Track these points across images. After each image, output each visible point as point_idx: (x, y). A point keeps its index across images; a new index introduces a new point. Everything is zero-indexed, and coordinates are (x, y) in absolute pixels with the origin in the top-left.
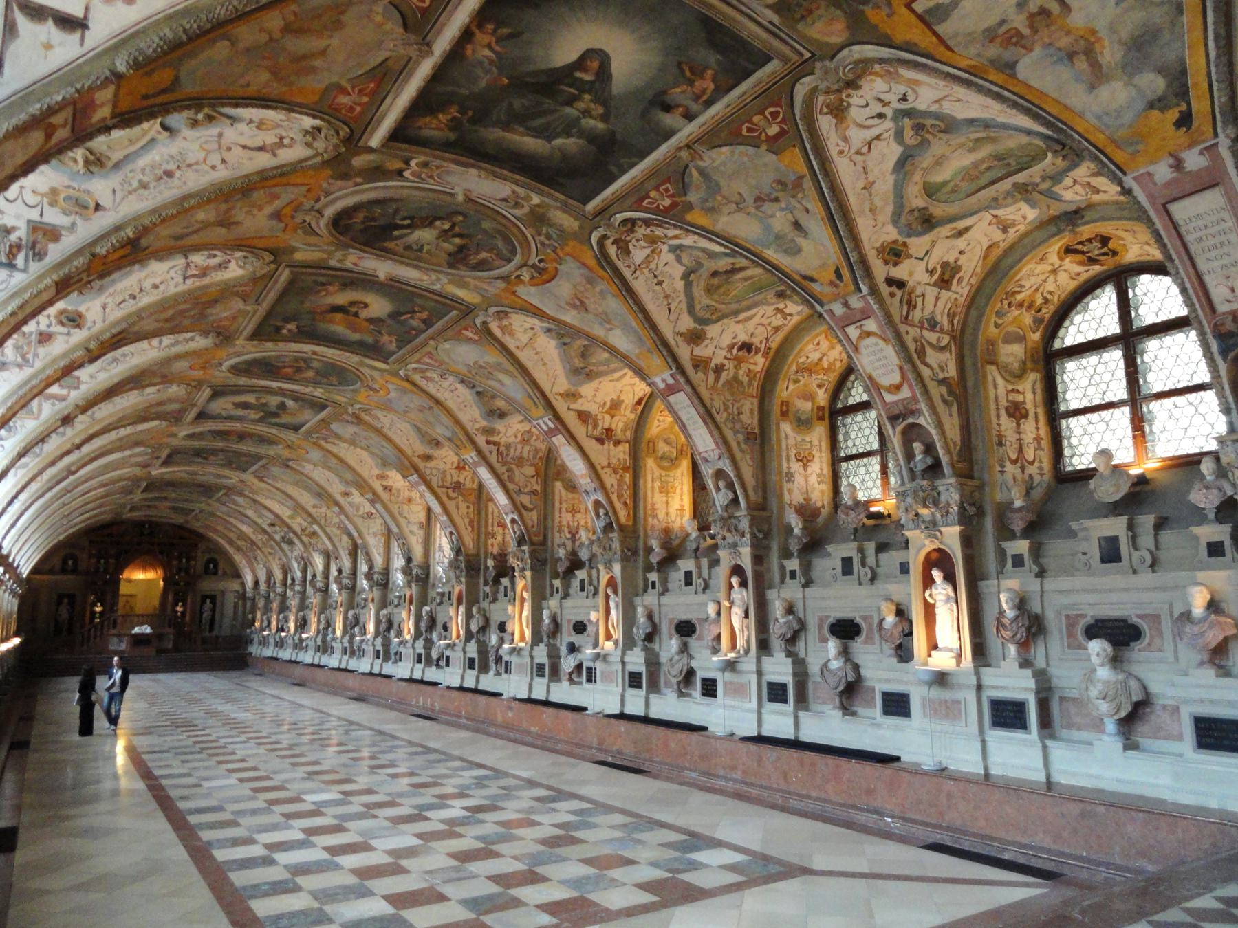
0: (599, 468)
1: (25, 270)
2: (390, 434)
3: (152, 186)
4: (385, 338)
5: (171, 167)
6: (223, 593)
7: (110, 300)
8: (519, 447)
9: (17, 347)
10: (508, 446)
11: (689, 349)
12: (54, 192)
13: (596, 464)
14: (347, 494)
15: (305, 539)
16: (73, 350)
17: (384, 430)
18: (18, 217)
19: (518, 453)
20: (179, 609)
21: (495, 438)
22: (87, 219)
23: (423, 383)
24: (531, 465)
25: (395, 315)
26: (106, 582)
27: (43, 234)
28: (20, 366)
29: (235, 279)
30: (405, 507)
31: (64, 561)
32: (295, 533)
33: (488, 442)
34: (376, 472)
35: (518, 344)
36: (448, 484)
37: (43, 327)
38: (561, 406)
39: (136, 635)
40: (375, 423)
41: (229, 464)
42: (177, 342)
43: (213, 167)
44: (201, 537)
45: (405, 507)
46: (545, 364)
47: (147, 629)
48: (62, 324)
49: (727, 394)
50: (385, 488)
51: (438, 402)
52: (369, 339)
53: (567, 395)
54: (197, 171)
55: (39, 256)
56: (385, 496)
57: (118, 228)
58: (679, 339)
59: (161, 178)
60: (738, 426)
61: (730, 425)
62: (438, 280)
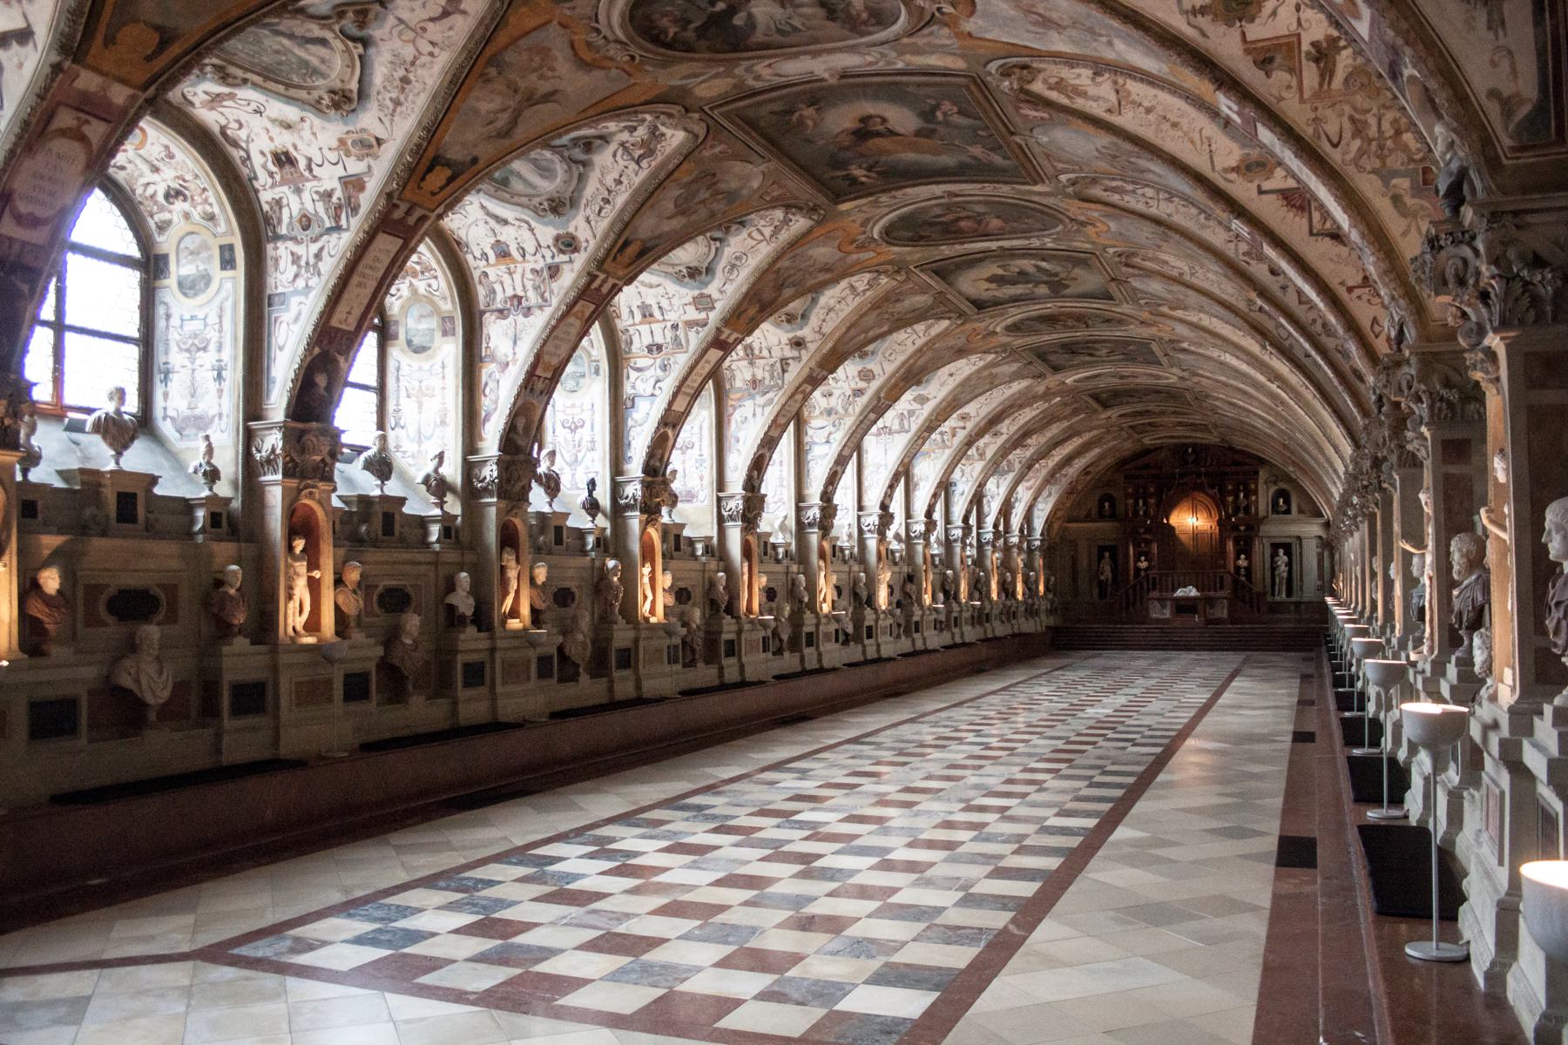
0: (1342, 292)
1: (347, 229)
2: (1194, 281)
3: (402, 98)
4: (977, 151)
5: (401, 73)
6: (1299, 538)
7: (588, 211)
9: (536, 288)
11: (1235, 33)
12: (342, 142)
13: (1333, 282)
17: (1187, 277)
18: (331, 178)
20: (1242, 562)
22: (376, 157)
23: (1115, 198)
25: (928, 115)
26: (1149, 530)
27: (353, 184)
28: (541, 308)
29: (681, 145)
31: (1101, 506)
35: (1106, 106)
37: (549, 261)
38: (1243, 190)
40: (1165, 269)
42: (777, 230)
43: (431, 54)
44: (1262, 462)
46: (1175, 125)
47: (1192, 592)
48: (563, 252)
49: (1360, 99)
51: (1157, 221)
52: (964, 158)
53: (1249, 168)
54: (424, 65)
55: (355, 210)
57: (401, 155)
58: (1202, 21)
59: (403, 89)
60: (1396, 161)
61: (1372, 163)
62: (883, 55)
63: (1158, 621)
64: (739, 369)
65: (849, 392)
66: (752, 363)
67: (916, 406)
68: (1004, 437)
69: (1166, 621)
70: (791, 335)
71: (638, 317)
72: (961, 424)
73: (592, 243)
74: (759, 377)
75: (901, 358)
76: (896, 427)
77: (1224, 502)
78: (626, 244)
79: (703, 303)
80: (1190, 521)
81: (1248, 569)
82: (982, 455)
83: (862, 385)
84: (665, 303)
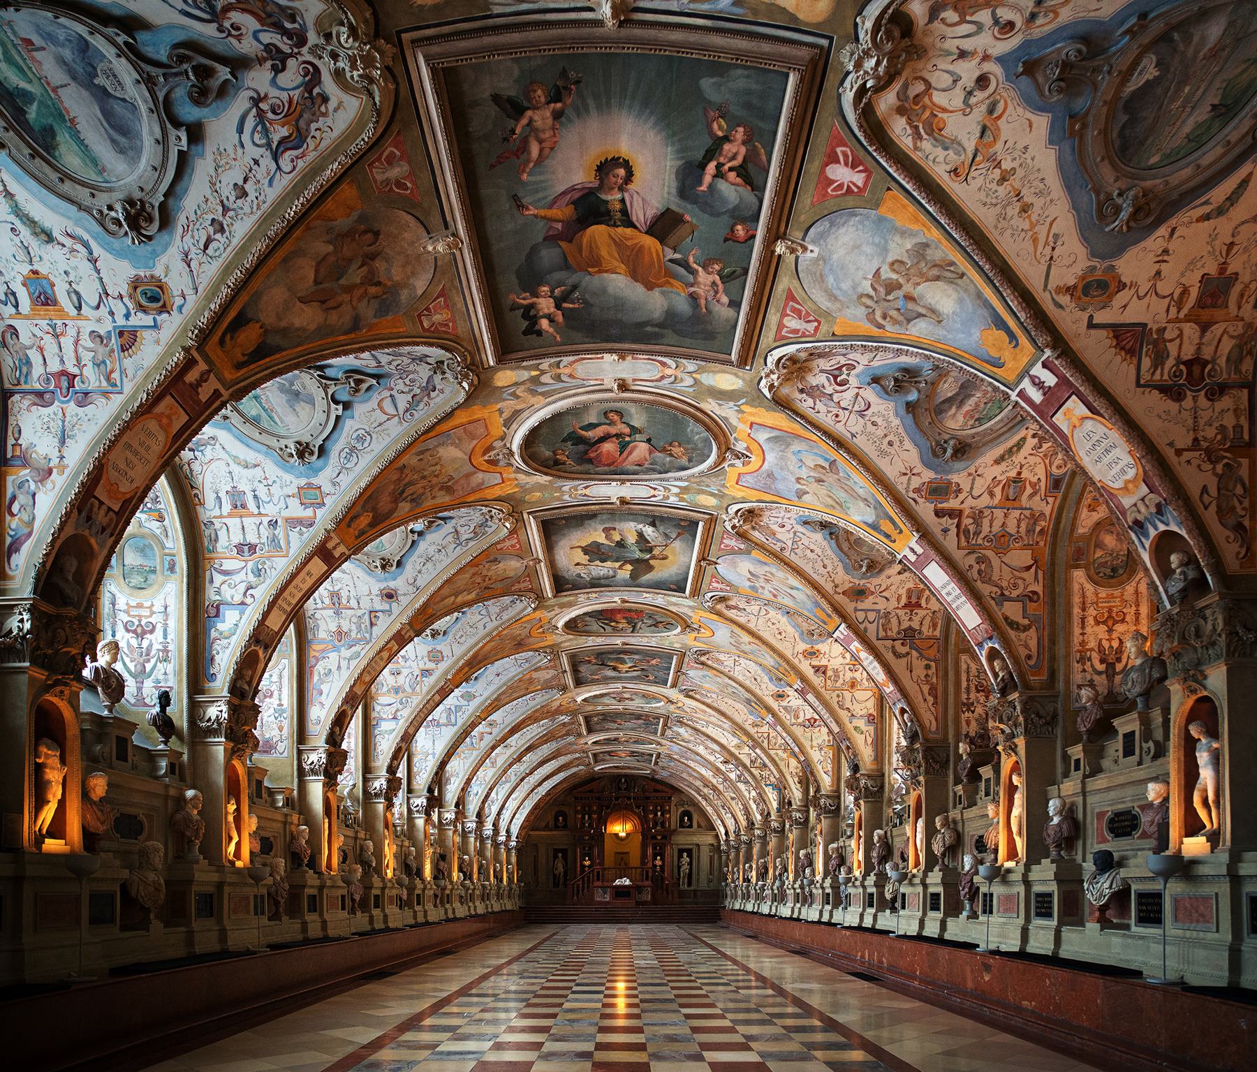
8: (999, 513)
10: (978, 516)
14: (780, 696)
15: (756, 772)
16: (169, 353)
19: (996, 528)
21: (953, 503)
24: (1025, 547)
30: (847, 695)
32: (745, 766)
33: (939, 513)
34: (802, 646)
36: (893, 634)
39: (617, 887)
41: (644, 678)
45: (847, 695)
50: (817, 669)
56: (817, 680)
63: (600, 903)
64: (323, 618)
65: (417, 672)
66: (337, 613)
67: (464, 702)
68: (513, 749)
69: (608, 903)
70: (383, 585)
71: (227, 508)
72: (488, 730)
73: (191, 299)
74: (345, 629)
75: (471, 641)
76: (443, 720)
77: (646, 817)
78: (241, 321)
79: (310, 495)
80: (619, 828)
81: (662, 867)
82: (493, 764)
83: (431, 665)
84: (262, 492)
